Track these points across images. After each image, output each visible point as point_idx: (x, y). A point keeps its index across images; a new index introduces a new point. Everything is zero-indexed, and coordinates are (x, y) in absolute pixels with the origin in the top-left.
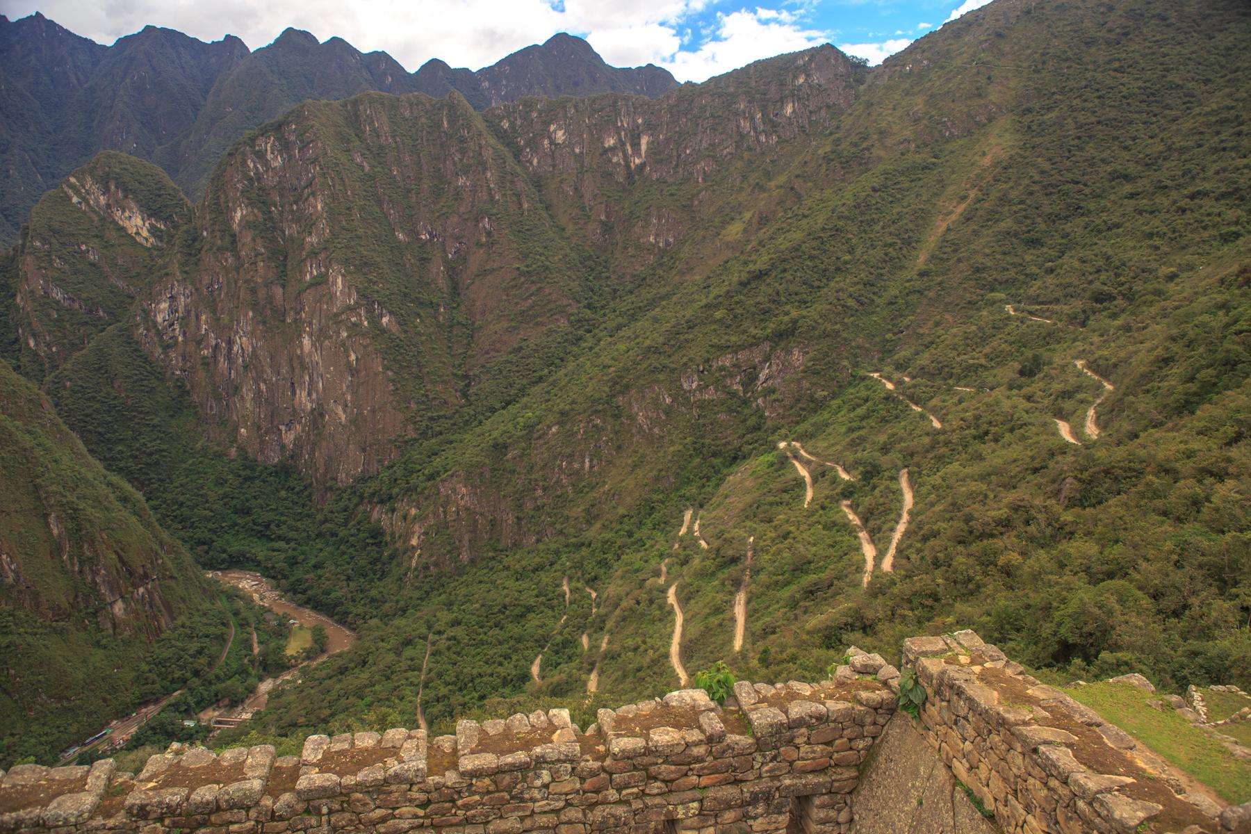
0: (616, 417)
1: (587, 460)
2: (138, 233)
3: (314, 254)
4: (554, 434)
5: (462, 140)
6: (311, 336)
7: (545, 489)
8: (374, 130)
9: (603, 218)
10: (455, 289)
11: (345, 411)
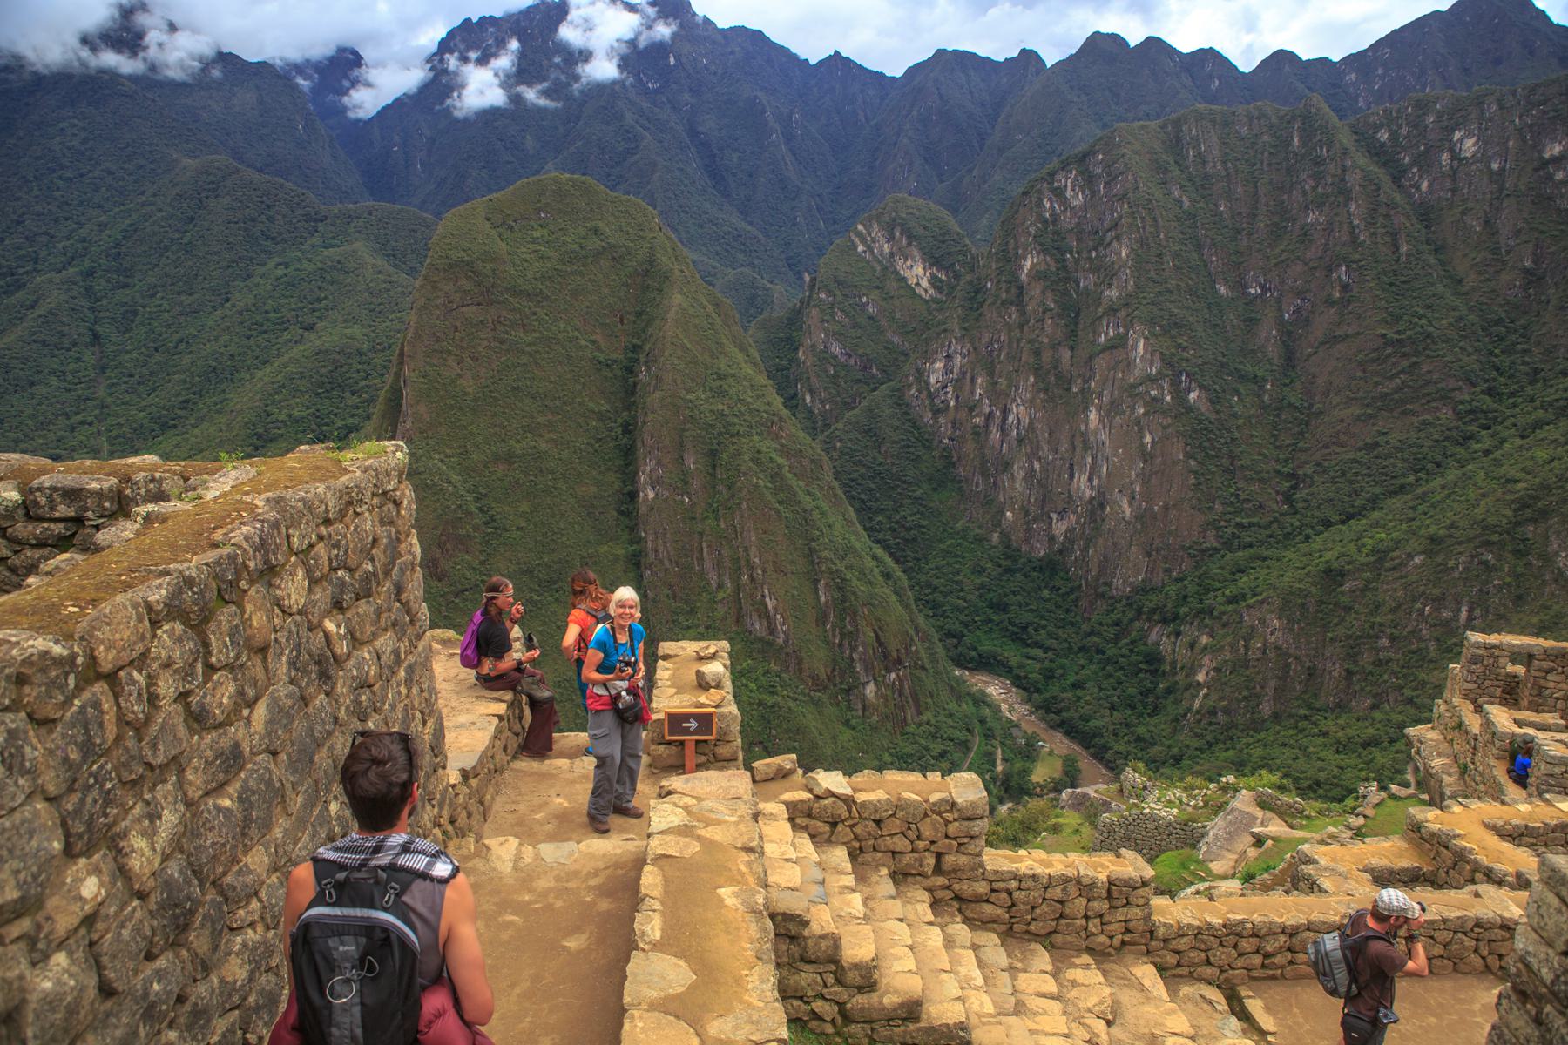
0: (1519, 554)
1: (1464, 609)
2: (918, 284)
3: (1112, 311)
4: (1416, 567)
5: (1318, 162)
6: (1099, 409)
7: (1393, 639)
8: (1199, 155)
9: (1528, 263)
10: (1290, 360)
11: (1130, 504)
